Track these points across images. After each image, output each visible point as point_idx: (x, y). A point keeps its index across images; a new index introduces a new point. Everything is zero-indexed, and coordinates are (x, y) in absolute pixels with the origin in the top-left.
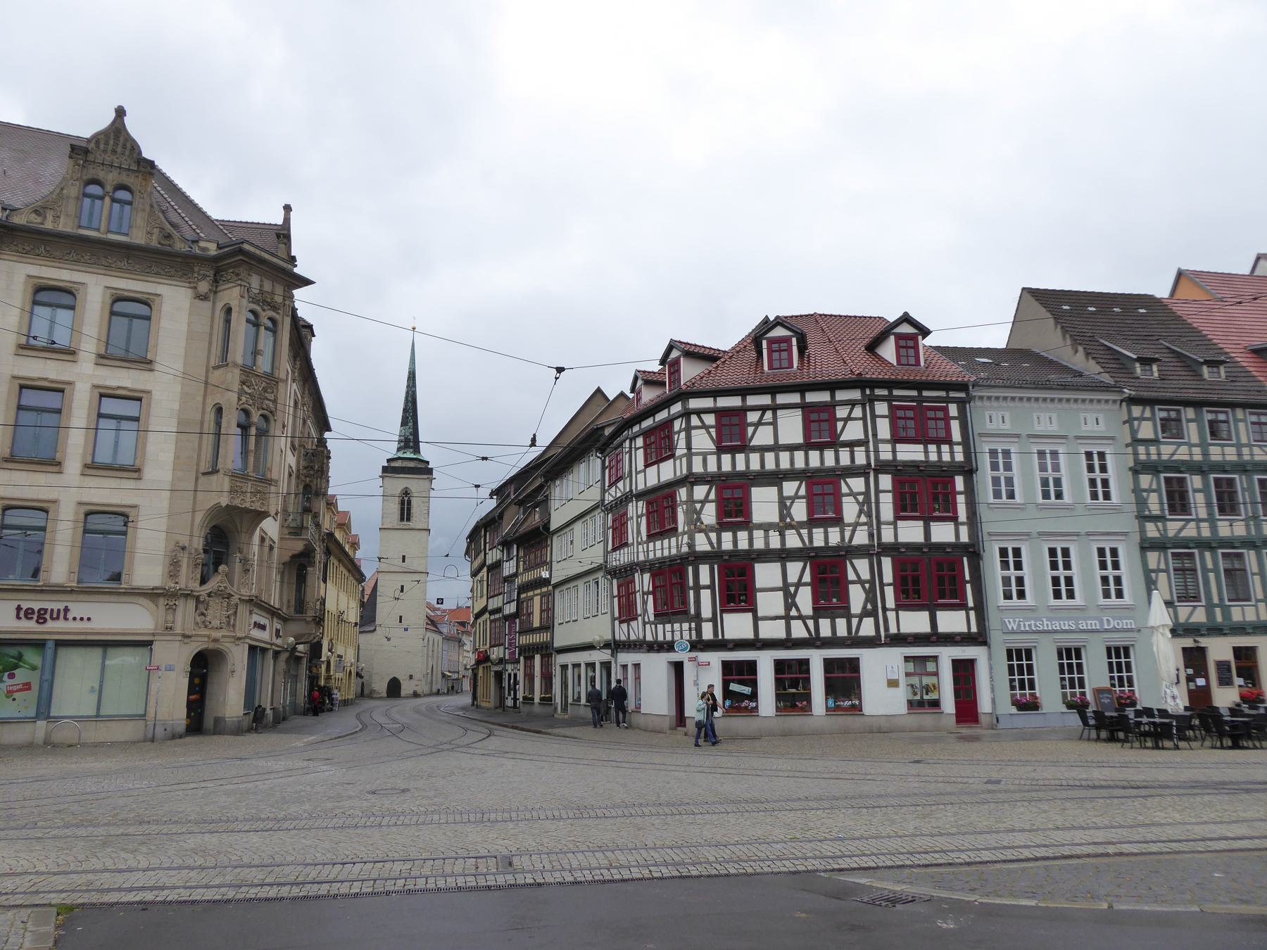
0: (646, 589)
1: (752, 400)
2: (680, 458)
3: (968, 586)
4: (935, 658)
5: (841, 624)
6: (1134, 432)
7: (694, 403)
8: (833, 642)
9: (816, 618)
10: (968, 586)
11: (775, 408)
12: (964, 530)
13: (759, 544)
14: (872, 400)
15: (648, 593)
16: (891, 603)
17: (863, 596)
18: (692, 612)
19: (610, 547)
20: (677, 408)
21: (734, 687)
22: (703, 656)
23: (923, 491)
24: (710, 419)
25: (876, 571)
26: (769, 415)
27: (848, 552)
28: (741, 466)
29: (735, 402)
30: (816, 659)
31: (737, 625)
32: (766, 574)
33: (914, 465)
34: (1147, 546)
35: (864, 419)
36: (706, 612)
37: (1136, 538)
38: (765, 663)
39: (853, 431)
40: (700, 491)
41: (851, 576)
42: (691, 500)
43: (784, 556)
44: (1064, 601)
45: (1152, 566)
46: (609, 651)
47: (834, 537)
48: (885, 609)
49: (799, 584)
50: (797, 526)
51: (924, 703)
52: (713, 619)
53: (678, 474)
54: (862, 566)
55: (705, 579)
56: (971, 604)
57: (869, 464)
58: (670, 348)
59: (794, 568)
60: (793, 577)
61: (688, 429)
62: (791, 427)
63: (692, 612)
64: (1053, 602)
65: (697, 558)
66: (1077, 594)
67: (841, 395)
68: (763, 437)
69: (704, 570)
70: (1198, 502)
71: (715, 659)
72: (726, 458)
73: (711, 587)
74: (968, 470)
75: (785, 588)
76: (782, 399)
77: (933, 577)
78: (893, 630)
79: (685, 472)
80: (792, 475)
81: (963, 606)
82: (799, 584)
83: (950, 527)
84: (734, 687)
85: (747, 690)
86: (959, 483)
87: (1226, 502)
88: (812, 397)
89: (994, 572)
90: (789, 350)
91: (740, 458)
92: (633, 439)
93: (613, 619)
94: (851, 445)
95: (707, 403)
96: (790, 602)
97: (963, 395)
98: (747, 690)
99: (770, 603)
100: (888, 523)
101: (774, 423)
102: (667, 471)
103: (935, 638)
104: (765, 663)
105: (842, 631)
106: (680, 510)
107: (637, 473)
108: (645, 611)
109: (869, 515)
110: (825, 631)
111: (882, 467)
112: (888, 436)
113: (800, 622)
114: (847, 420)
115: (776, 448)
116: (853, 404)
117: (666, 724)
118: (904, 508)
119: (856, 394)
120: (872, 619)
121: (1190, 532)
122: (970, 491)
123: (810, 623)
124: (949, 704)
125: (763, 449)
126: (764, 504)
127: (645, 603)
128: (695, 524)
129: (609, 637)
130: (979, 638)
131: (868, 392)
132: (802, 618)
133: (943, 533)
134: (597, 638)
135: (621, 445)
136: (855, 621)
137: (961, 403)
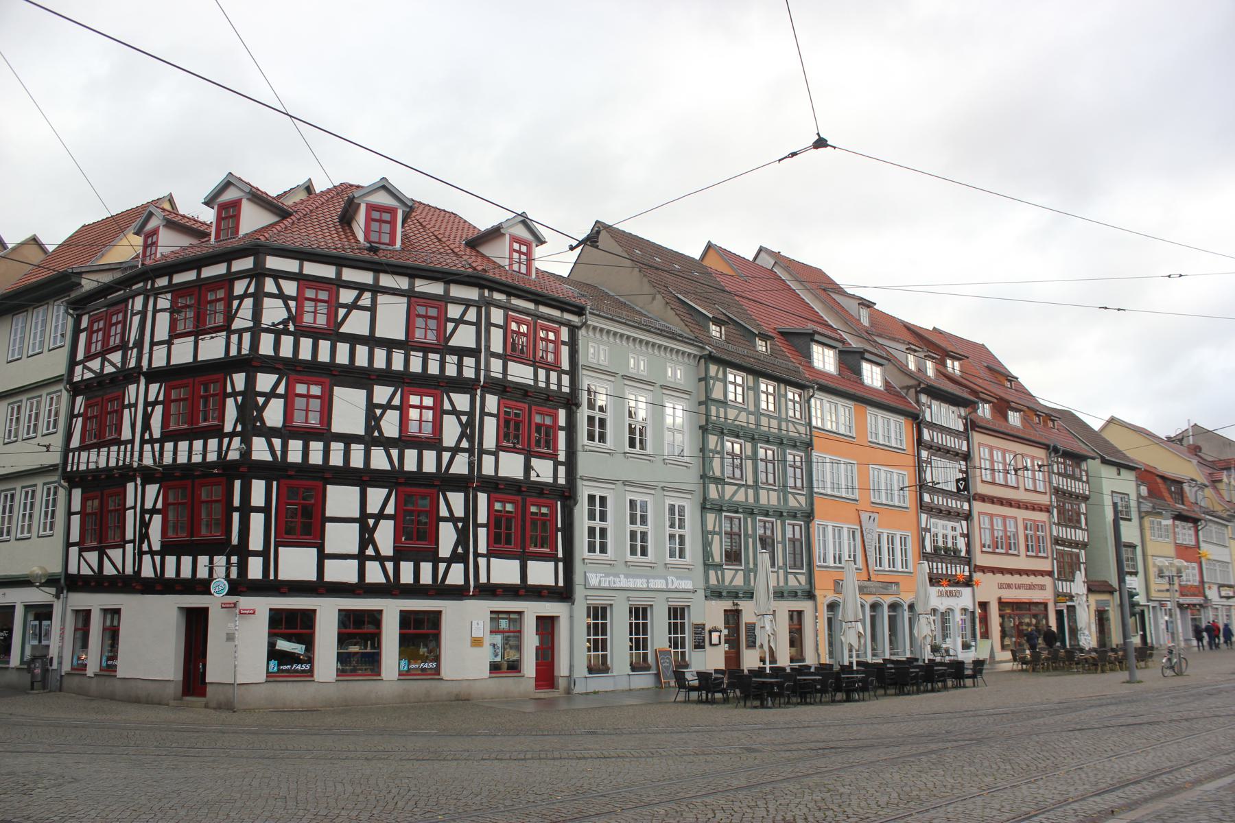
0: (149, 505)
1: (349, 275)
2: (240, 332)
3: (559, 534)
4: (520, 613)
5: (426, 568)
6: (708, 391)
7: (273, 263)
8: (416, 590)
9: (397, 558)
10: (559, 534)
11: (376, 290)
12: (562, 470)
13: (336, 459)
14: (490, 303)
15: (154, 511)
16: (482, 548)
17: (454, 537)
18: (235, 540)
19: (75, 443)
20: (247, 263)
21: (283, 645)
22: (245, 602)
25: (471, 506)
26: (366, 300)
27: (445, 482)
28: (324, 356)
29: (328, 271)
30: (391, 610)
31: (296, 563)
32: (341, 500)
34: (706, 506)
35: (477, 324)
36: (256, 542)
37: (698, 498)
38: (327, 612)
39: (464, 337)
40: (265, 382)
41: (444, 512)
42: (250, 390)
43: (364, 478)
44: (639, 557)
45: (710, 528)
46: (53, 590)
47: (430, 466)
48: (477, 555)
49: (381, 516)
50: (387, 443)
51: (506, 667)
52: (264, 554)
53: (233, 352)
54: (457, 500)
55: (258, 499)
56: (560, 555)
57: (477, 378)
58: (227, 184)
59: (376, 496)
60: (373, 508)
61: (258, 297)
62: (392, 318)
63: (235, 540)
64: (629, 557)
65: (248, 469)
66: (650, 550)
67: (457, 291)
68: (357, 324)
69: (258, 489)
71: (263, 605)
72: (306, 344)
73: (266, 510)
74: (571, 403)
75: (364, 517)
76: (386, 280)
78: (483, 579)
79: (245, 351)
80: (387, 377)
81: (551, 557)
82: (381, 516)
83: (549, 464)
84: (283, 645)
85: (299, 649)
88: (422, 286)
90: (392, 223)
91: (325, 345)
92: (157, 292)
93: (68, 545)
94: (461, 352)
95: (291, 265)
96: (367, 537)
97: (574, 319)
98: (299, 649)
99: (342, 538)
100: (489, 453)
101: (372, 309)
102: (213, 348)
103: (524, 591)
104: (327, 612)
105: (426, 578)
106: (230, 402)
107: (153, 344)
108: (144, 536)
109: (471, 440)
110: (407, 576)
112: (500, 351)
113: (377, 564)
114: (460, 321)
115: (372, 341)
116: (467, 304)
117: (174, 690)
119: (472, 294)
120: (461, 566)
122: (571, 428)
123: (390, 566)
124: (529, 667)
125: (354, 340)
127: (145, 525)
128: (251, 424)
129: (56, 568)
130: (564, 593)
131: (486, 293)
132: (378, 557)
133: (543, 471)
134: (36, 570)
135: (125, 301)
136: (442, 566)
137: (573, 330)
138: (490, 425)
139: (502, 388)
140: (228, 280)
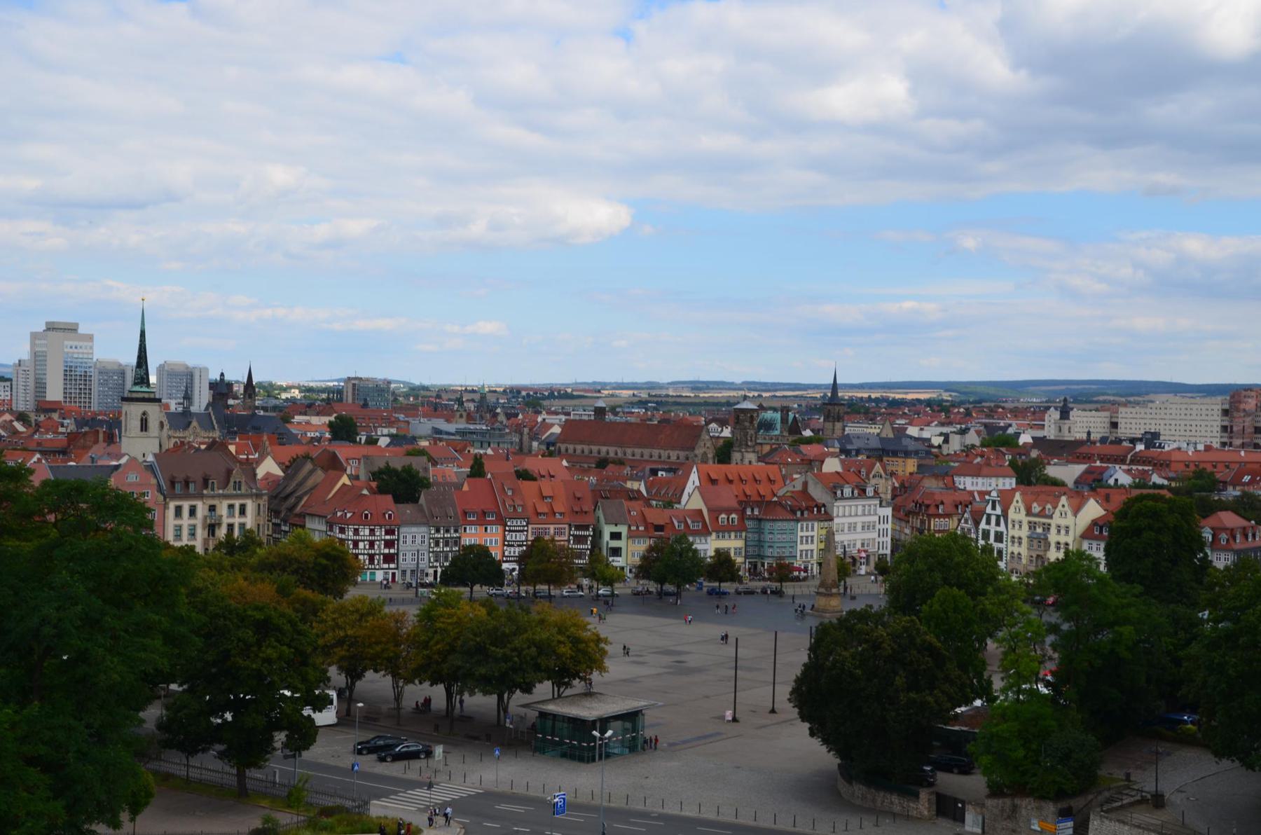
23: (389, 544)
62: (367, 532)
77: (389, 559)
87: (447, 544)
89: (401, 557)
126: (361, 545)
133: (392, 551)
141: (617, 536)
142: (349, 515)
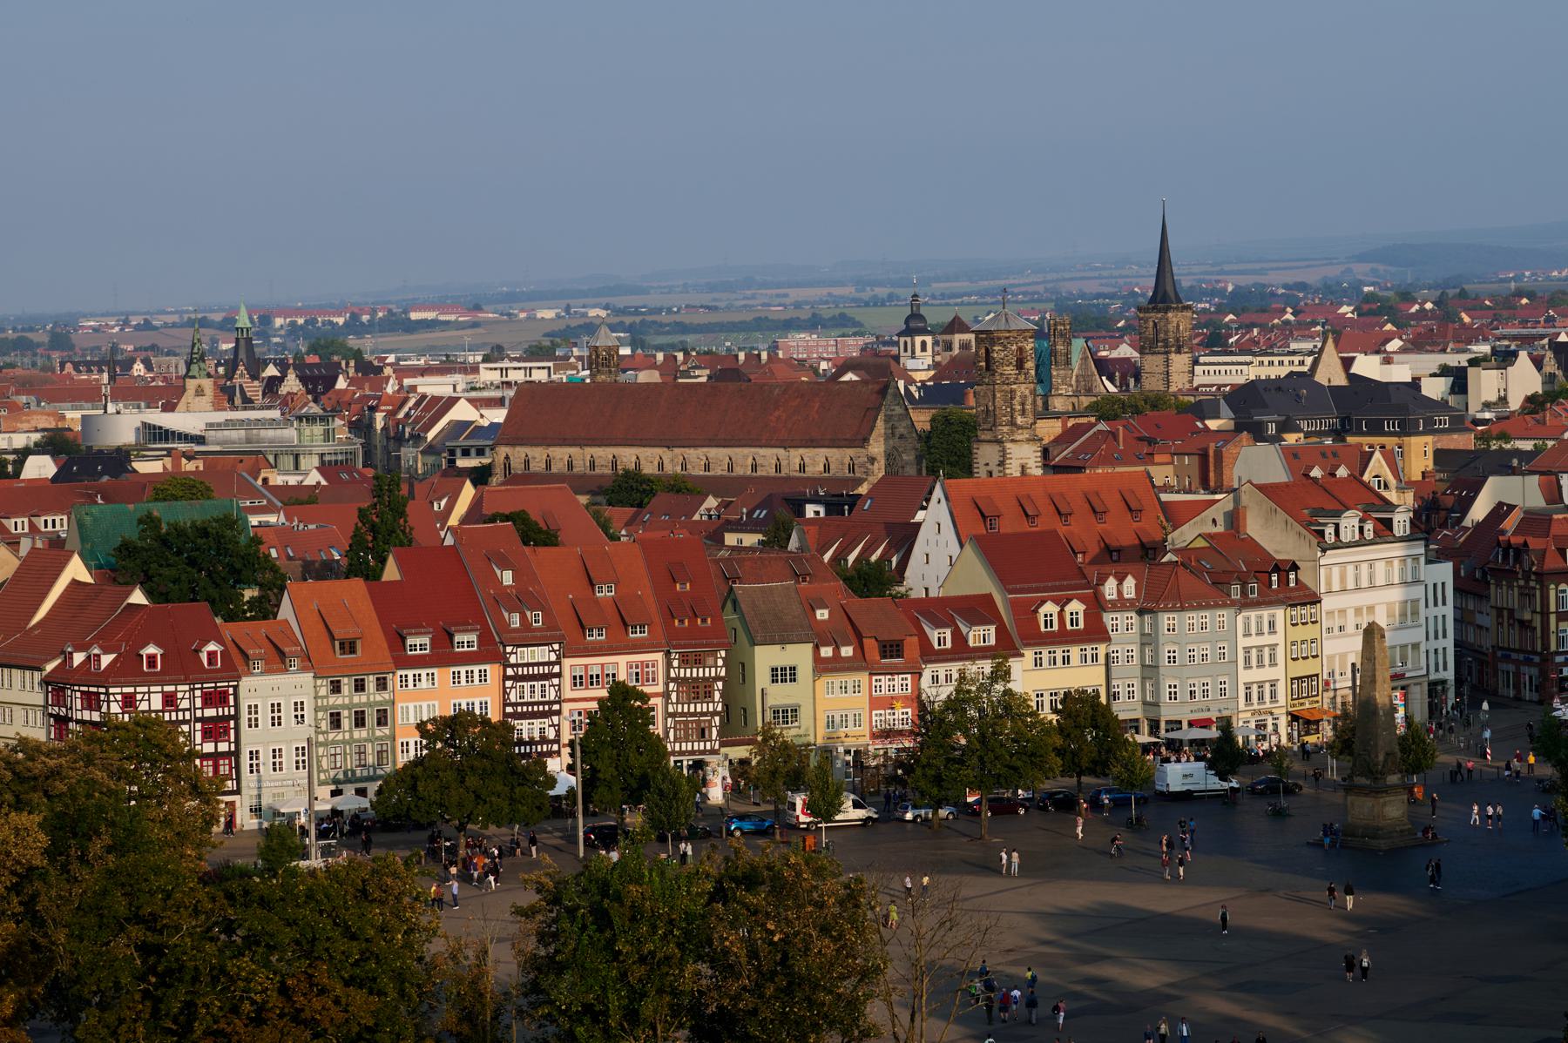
7: (111, 690)
20: (102, 690)
24: (119, 697)
29: (131, 690)
33: (211, 718)
39: (185, 704)
61: (109, 702)
70: (345, 723)
74: (236, 717)
86: (232, 723)
94: (184, 710)
111: (197, 720)
118: (207, 735)
121: (340, 737)
133: (223, 747)
138: (199, 735)
139: (202, 720)
140: (98, 694)
141: (783, 675)
142: (106, 660)
